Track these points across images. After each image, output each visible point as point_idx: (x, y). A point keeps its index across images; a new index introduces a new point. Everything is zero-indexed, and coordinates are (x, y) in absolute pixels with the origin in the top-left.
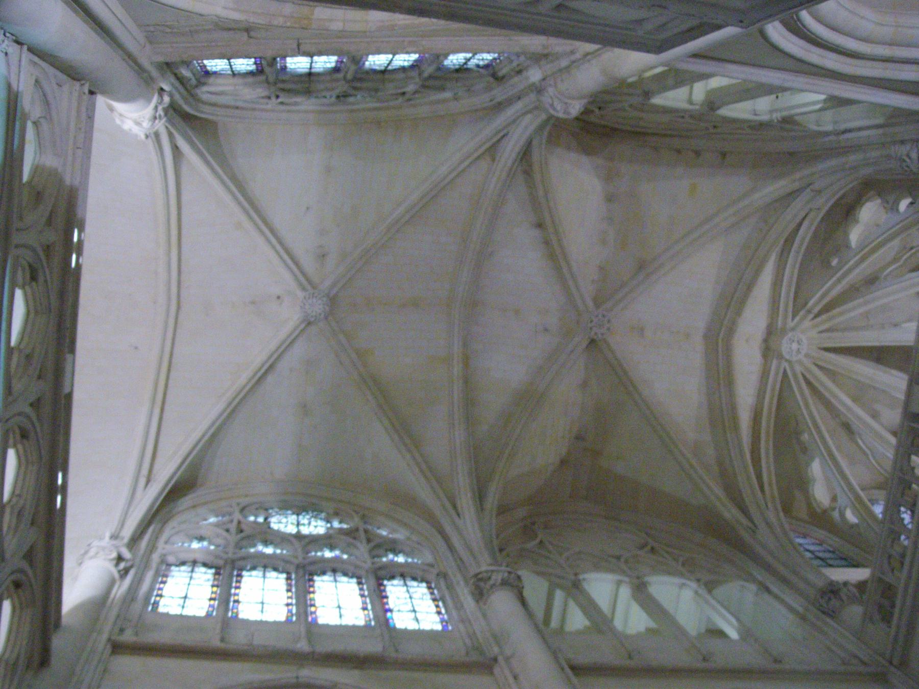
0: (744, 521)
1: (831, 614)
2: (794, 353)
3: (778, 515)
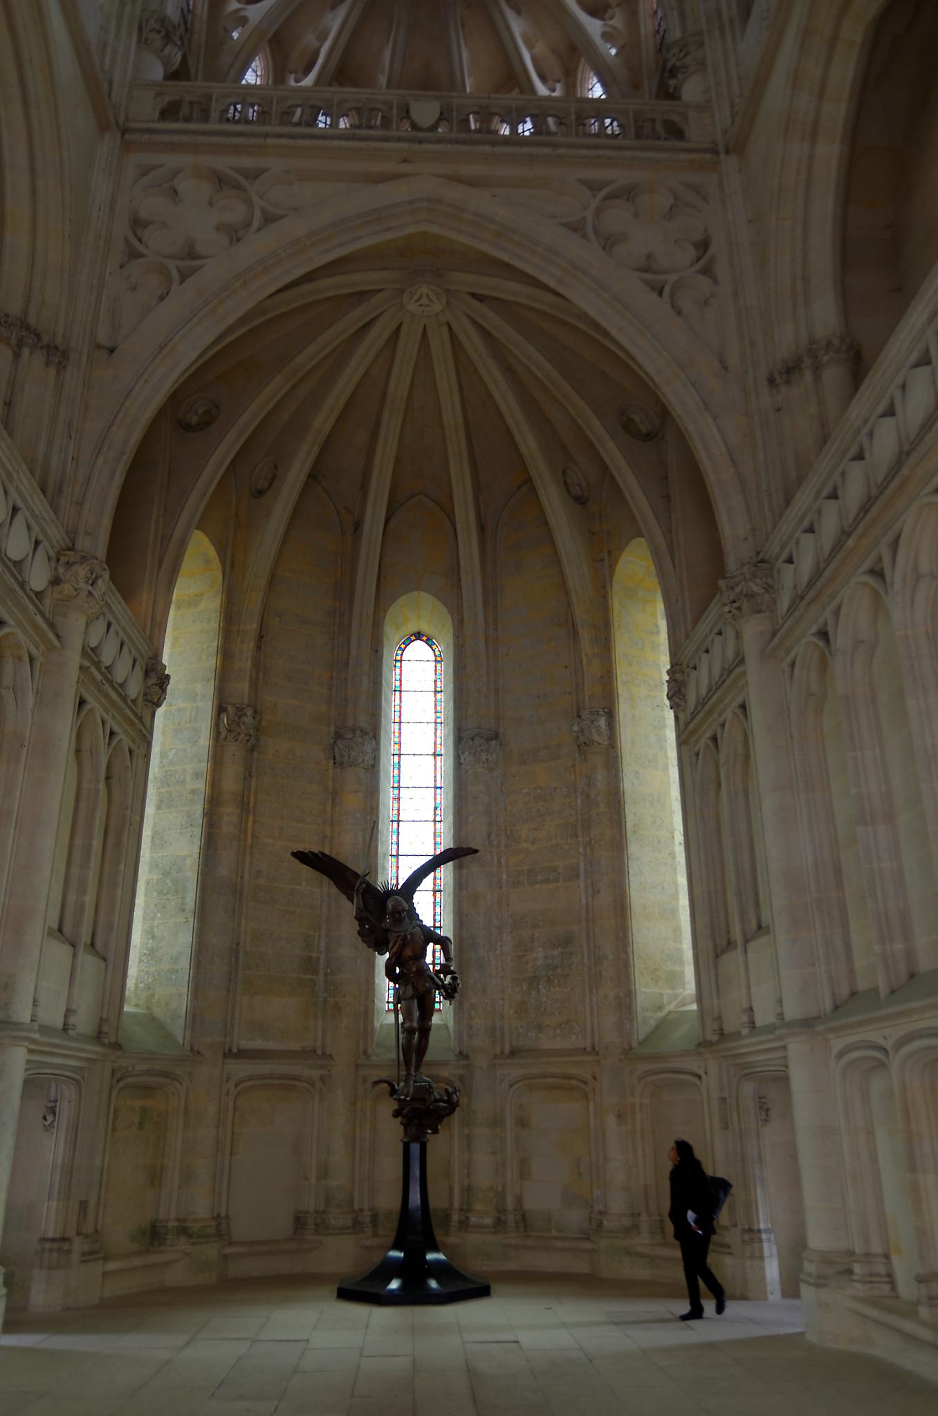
1: (143, 42)
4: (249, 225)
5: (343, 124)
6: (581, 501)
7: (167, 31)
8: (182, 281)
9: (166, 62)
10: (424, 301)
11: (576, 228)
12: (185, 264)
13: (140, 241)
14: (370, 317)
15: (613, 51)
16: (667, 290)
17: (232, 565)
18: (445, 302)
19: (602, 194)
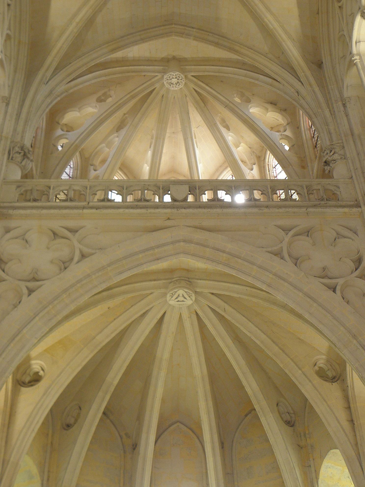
0: (49, 74)
1: (10, 158)
2: (169, 81)
3: (58, 96)
4: (72, 259)
5: (130, 198)
6: (290, 424)
7: (25, 152)
8: (29, 295)
9: (23, 168)
10: (181, 298)
11: (278, 254)
12: (31, 285)
13: (4, 271)
14: (147, 309)
15: (287, 148)
16: (338, 288)
17: (48, 480)
18: (194, 298)
19: (291, 233)
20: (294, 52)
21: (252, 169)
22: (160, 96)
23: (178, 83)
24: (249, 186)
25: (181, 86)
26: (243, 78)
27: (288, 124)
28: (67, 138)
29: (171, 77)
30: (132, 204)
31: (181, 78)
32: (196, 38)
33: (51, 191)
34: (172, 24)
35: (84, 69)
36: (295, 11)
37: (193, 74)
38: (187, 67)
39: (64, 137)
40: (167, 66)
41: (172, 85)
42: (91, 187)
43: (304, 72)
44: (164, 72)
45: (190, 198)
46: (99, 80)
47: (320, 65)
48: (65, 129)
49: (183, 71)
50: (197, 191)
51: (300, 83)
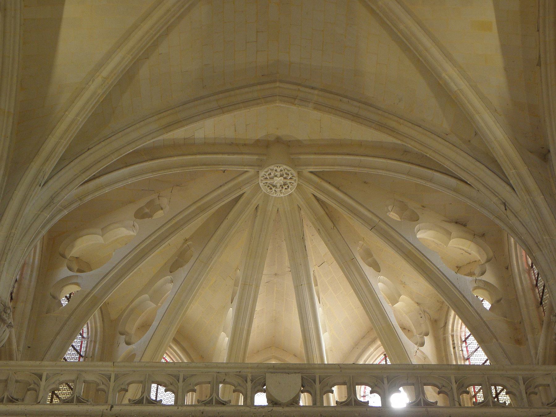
2: (269, 182)
3: (65, 207)
5: (190, 399)
15: (487, 305)
20: (496, 132)
21: (422, 344)
22: (252, 207)
23: (285, 184)
24: (415, 377)
25: (290, 191)
26: (404, 177)
27: (488, 261)
28: (77, 284)
29: (272, 175)
30: (193, 409)
31: (290, 176)
32: (318, 106)
33: (43, 383)
34: (275, 81)
35: (115, 158)
36: (498, 61)
37: (312, 169)
38: (302, 157)
39: (74, 281)
40: (266, 155)
41: (274, 189)
42: (117, 377)
43: (515, 168)
44: (261, 165)
45: (304, 400)
46: (140, 178)
47: (544, 155)
48: (76, 268)
49: (294, 164)
50: (318, 386)
51: (508, 188)
